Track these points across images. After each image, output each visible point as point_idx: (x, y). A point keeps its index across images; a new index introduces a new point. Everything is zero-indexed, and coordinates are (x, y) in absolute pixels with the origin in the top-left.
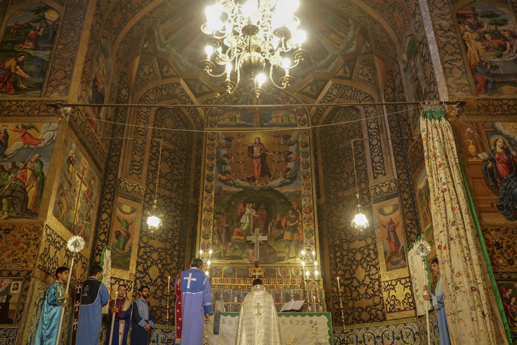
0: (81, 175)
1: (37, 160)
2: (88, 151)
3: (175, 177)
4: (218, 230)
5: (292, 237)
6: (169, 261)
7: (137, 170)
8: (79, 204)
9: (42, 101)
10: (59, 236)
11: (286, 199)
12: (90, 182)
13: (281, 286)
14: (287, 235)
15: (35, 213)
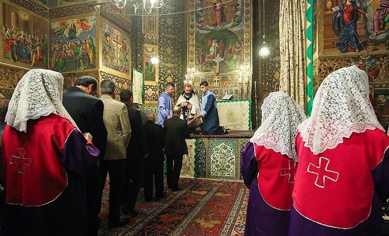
0: (116, 40)
1: (90, 38)
2: (118, 25)
3: (176, 26)
4: (198, 57)
5: (238, 58)
6: (177, 73)
7: (153, 27)
8: (118, 55)
9: (85, 3)
10: (109, 74)
11: (235, 35)
12: (123, 42)
13: (230, 86)
14: (235, 57)
15: (94, 65)
